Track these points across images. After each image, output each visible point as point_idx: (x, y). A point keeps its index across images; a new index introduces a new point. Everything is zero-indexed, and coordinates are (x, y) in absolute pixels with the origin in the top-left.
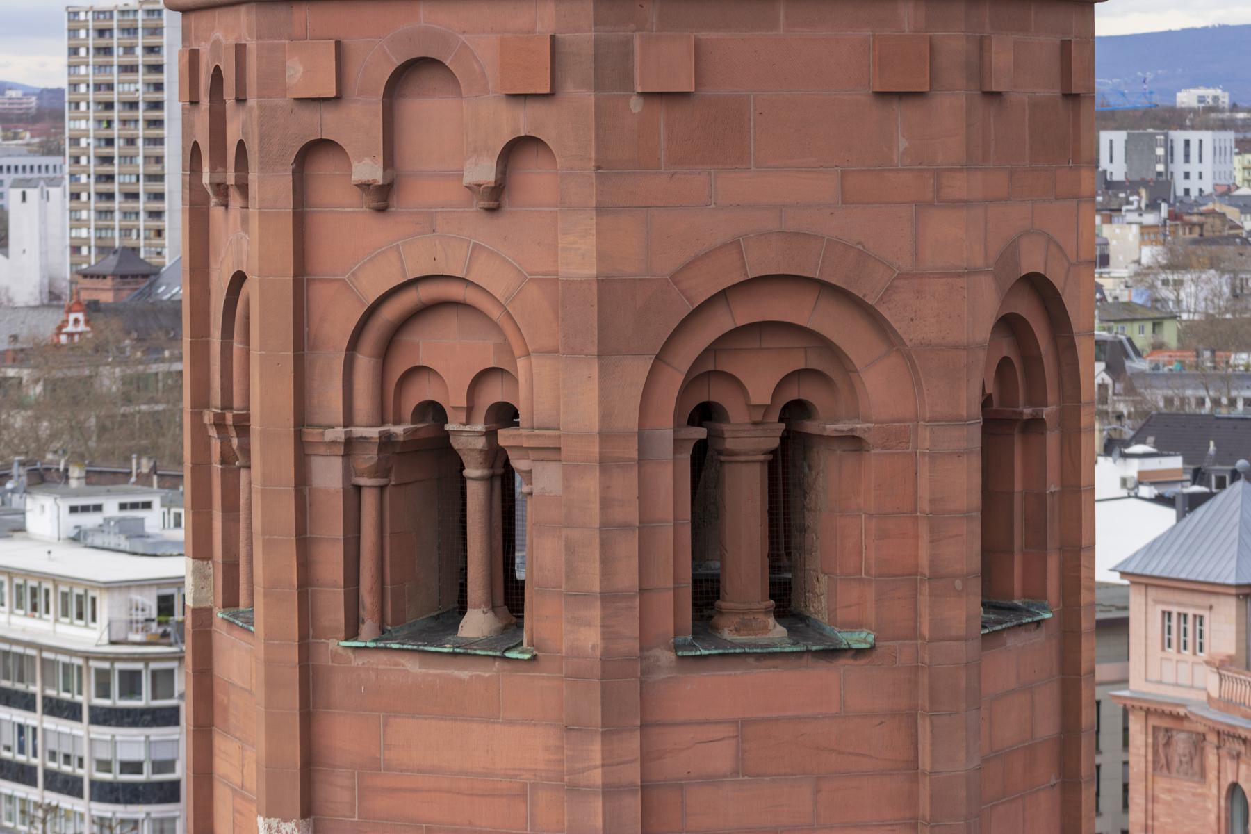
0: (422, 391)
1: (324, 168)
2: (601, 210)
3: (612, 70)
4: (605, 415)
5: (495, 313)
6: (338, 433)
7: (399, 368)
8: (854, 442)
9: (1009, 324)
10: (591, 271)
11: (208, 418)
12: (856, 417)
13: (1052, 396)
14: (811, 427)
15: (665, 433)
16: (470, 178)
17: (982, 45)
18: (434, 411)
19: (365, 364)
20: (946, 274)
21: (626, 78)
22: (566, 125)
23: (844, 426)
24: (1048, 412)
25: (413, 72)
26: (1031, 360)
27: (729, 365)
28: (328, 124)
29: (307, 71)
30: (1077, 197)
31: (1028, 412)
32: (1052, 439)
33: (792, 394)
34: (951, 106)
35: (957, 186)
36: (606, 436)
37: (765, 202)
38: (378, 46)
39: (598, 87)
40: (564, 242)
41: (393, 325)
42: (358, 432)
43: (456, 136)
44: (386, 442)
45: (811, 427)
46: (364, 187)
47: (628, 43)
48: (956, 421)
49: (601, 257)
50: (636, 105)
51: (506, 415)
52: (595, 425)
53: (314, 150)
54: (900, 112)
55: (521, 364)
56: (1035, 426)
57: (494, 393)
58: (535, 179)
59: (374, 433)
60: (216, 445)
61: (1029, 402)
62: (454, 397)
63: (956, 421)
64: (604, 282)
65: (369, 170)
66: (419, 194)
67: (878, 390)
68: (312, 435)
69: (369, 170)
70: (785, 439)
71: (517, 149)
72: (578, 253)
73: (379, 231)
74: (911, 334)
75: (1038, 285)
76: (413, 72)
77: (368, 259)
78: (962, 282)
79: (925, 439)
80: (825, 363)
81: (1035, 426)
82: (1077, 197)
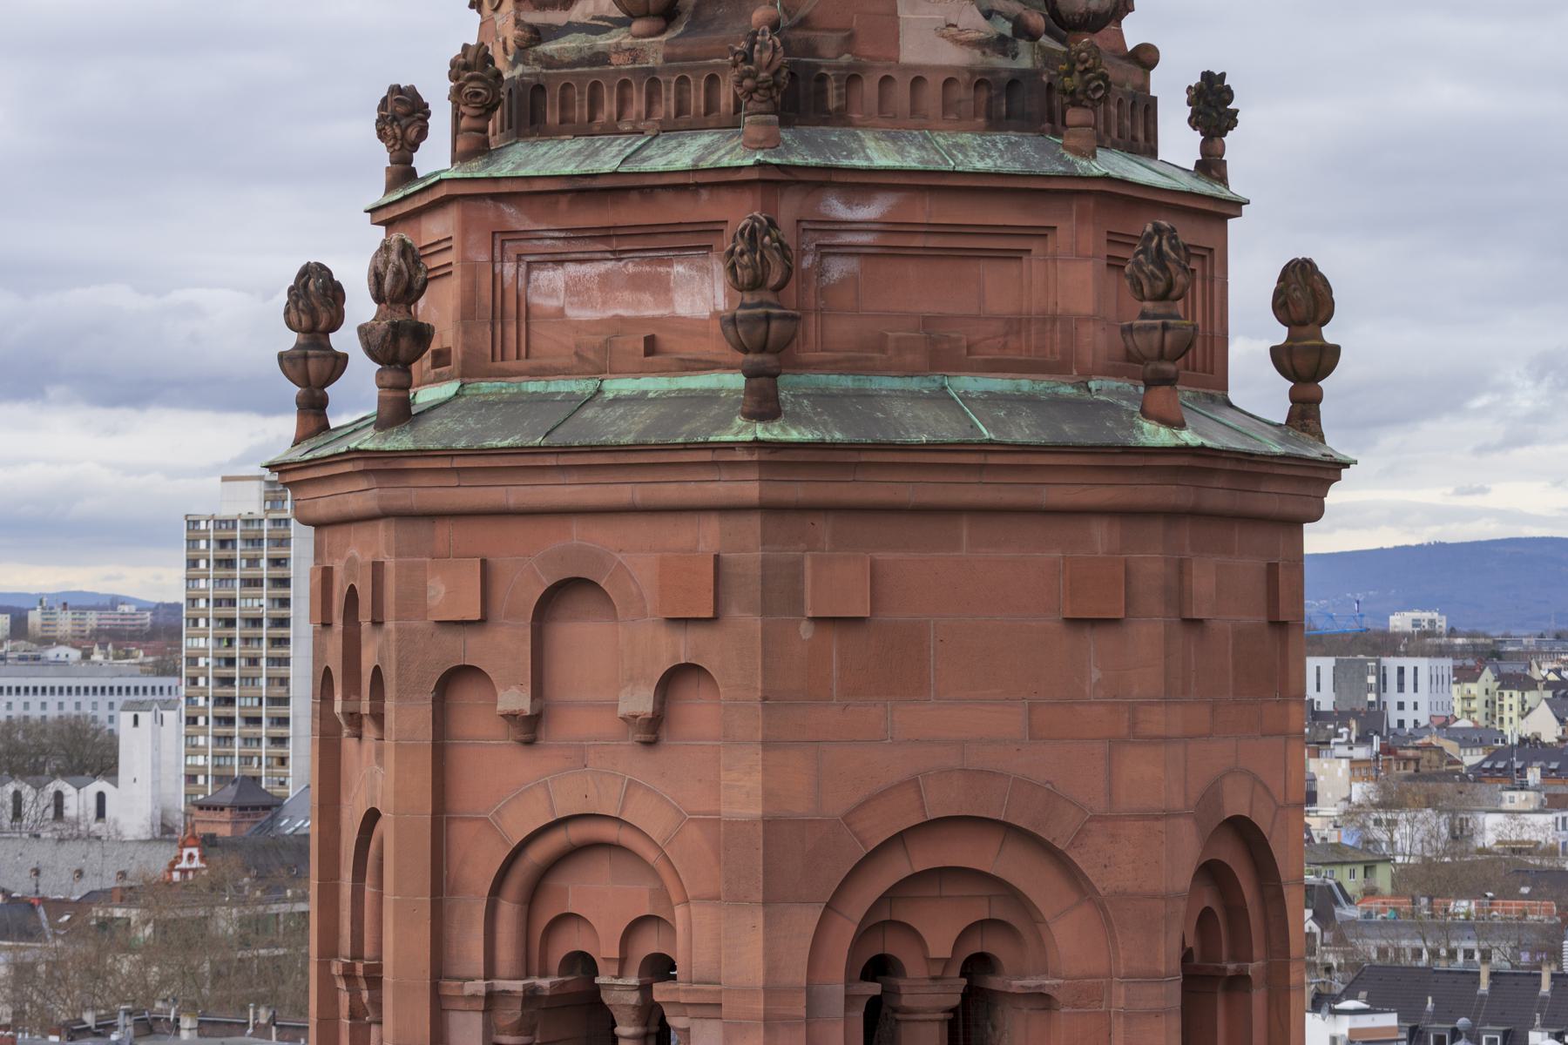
0: (570, 941)
1: (467, 697)
2: (767, 744)
3: (780, 593)
4: (771, 969)
5: (651, 856)
6: (479, 987)
7: (545, 916)
8: (1042, 1000)
9: (1211, 872)
10: (755, 811)
11: (336, 968)
12: (1045, 972)
13: (1257, 952)
14: (994, 983)
15: (835, 986)
16: (625, 709)
17: (1182, 568)
18: (583, 963)
19: (508, 910)
20: (1143, 817)
21: (796, 602)
22: (730, 652)
23: (1031, 982)
24: (1254, 968)
25: (566, 593)
26: (1236, 912)
27: (904, 914)
28: (471, 650)
29: (449, 591)
30: (1285, 734)
31: (1231, 967)
32: (1258, 997)
33: (975, 946)
34: (1148, 635)
35: (1156, 721)
36: (770, 991)
37: (948, 738)
38: (526, 569)
39: (766, 610)
40: (727, 780)
41: (542, 868)
42: (501, 985)
43: (610, 664)
44: (531, 995)
45: (994, 983)
46: (510, 717)
47: (798, 564)
48: (1153, 978)
49: (768, 795)
50: (806, 631)
51: (662, 967)
52: (758, 978)
53: (457, 677)
54: (1093, 641)
55: (679, 912)
56: (1239, 982)
57: (650, 944)
58: (697, 712)
59: (517, 986)
60: (344, 999)
61: (1234, 958)
62: (605, 948)
63: (1153, 978)
64: (770, 823)
65: (516, 699)
66: (570, 726)
67: (1069, 943)
68: (450, 988)
69: (516, 699)
70: (966, 996)
71: (677, 677)
72: (743, 792)
73: (522, 766)
74: (1104, 884)
75: (1243, 830)
76: (566, 593)
77: (515, 796)
78: (1160, 825)
79: (1120, 997)
80: (1011, 912)
81: (1239, 982)
82: (1285, 734)
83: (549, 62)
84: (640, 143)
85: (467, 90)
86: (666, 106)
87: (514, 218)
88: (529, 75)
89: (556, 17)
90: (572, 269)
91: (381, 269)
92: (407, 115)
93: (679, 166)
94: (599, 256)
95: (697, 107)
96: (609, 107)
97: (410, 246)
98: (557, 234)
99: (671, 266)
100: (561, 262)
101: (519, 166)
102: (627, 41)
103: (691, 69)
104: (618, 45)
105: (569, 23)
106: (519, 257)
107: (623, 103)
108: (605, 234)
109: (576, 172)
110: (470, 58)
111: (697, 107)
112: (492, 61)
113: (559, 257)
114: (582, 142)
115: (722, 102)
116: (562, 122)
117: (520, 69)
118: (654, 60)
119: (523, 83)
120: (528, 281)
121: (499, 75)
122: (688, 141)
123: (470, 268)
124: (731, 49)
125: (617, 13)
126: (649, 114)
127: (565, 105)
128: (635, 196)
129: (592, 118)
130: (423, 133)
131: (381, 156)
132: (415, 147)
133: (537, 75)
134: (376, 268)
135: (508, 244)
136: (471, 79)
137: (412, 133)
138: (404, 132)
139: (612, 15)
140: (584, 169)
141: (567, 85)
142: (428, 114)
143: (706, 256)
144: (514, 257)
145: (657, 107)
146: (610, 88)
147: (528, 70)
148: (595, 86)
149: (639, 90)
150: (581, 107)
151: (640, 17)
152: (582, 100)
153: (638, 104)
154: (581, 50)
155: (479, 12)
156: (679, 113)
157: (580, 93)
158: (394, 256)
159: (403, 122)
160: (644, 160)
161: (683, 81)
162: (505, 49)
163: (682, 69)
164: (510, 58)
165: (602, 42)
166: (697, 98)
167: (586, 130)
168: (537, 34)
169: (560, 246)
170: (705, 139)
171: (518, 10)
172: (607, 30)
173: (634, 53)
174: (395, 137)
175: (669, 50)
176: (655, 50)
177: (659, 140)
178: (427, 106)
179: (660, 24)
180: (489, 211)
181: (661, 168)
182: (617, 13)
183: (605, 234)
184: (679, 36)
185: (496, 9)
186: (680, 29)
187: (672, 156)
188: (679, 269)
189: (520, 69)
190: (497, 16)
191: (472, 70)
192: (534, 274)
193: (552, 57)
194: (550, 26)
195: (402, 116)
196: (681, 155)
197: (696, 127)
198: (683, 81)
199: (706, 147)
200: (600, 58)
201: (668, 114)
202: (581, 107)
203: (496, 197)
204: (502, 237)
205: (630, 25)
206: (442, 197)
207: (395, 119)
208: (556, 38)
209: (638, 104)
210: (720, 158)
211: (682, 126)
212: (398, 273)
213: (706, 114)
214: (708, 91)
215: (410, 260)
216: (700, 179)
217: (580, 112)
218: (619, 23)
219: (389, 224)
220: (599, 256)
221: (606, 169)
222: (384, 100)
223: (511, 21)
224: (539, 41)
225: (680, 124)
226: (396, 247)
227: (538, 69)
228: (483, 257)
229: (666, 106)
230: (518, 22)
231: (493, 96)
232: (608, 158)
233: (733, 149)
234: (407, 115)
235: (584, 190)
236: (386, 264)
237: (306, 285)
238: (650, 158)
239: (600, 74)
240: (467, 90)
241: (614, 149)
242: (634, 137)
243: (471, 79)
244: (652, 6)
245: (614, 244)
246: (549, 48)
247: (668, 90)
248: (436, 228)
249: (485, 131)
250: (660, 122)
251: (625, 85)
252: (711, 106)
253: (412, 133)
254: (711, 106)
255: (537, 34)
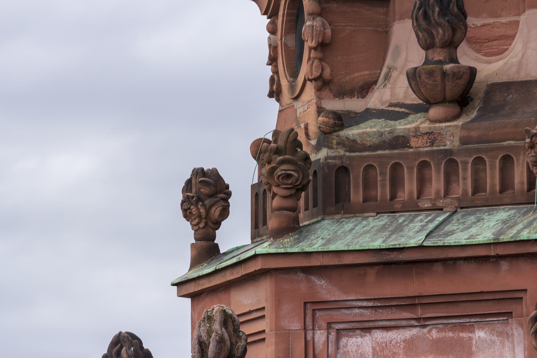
83: (352, 145)
84: (440, 219)
85: (279, 172)
86: (464, 184)
87: (325, 289)
88: (334, 158)
89: (354, 105)
90: (379, 335)
91: (204, 338)
92: (211, 196)
93: (480, 239)
94: (404, 323)
95: (493, 185)
96: (409, 186)
97: (231, 316)
98: (365, 304)
99: (473, 331)
100: (368, 330)
101: (329, 242)
102: (426, 126)
103: (487, 151)
104: (417, 129)
105: (368, 110)
106: (329, 325)
107: (422, 182)
108: (410, 303)
109: (384, 246)
110: (281, 143)
111: (493, 185)
112: (300, 145)
113: (367, 325)
114: (384, 219)
115: (517, 180)
116: (365, 201)
117: (324, 153)
118: (451, 143)
119: (328, 166)
120: (338, 348)
121: (307, 158)
122: (485, 216)
123: (283, 336)
124: (528, 132)
125: (413, 99)
126: (447, 193)
127: (368, 184)
128: (438, 268)
129: (393, 197)
130: (225, 213)
131: (186, 234)
132: (217, 224)
133: (341, 158)
134: (200, 337)
135: (318, 314)
136: (283, 162)
137: (216, 212)
138: (208, 211)
139: (408, 102)
140: (392, 243)
141: (370, 166)
142: (229, 194)
143: (506, 323)
144: (324, 325)
145: (454, 185)
146: (410, 169)
147: (332, 153)
148: (396, 168)
149: (438, 171)
150: (383, 186)
151: (437, 103)
152: (384, 180)
153: (436, 183)
154: (381, 134)
155: (278, 100)
156: (476, 191)
157: (383, 174)
158: (216, 326)
159: (207, 202)
160: (447, 234)
161: (479, 161)
162: (307, 134)
163: (478, 150)
164: (313, 142)
165: (402, 127)
166: (493, 177)
167: (388, 207)
168: (341, 120)
169: (368, 314)
170: (502, 214)
171: (319, 98)
172: (404, 116)
173: (432, 137)
174: (200, 216)
175: (465, 133)
176: (452, 132)
177: (455, 217)
178: (227, 187)
179: (455, 109)
180: (301, 285)
181: (464, 242)
182: (413, 99)
183: (410, 303)
184: (473, 121)
185: (297, 98)
186: (474, 114)
187: (473, 230)
188: (480, 334)
189: (324, 153)
190: (297, 104)
191: (277, 154)
192: (344, 341)
193: (354, 141)
194: (349, 112)
195: (205, 197)
196: (483, 228)
197: (493, 204)
198: (479, 161)
199: (504, 222)
200: (400, 142)
201: (465, 192)
202: (383, 186)
203: (308, 270)
204: (314, 306)
205: (426, 110)
206: (250, 273)
207: (199, 199)
208: (357, 123)
209: (436, 183)
210: (519, 232)
211: (478, 203)
212: (221, 341)
213: (501, 192)
214: (503, 170)
215: (231, 329)
216: (501, 251)
217: (382, 190)
218: (415, 109)
219: (194, 296)
220: (404, 323)
221: (413, 243)
222: (189, 183)
223: (313, 109)
224: (342, 127)
225: (478, 200)
226: (218, 318)
227: (341, 152)
228: (296, 326)
229: (464, 184)
230: (320, 110)
231: (300, 179)
232: (413, 233)
233: (530, 224)
234: (211, 196)
235: (391, 263)
236: (209, 333)
237: (119, 353)
238: (452, 233)
239: (400, 156)
240: (279, 172)
241: (417, 225)
242: (434, 214)
243: (283, 162)
244: (448, 94)
245: (420, 312)
246: (352, 132)
247: (465, 170)
248: (243, 301)
249: (294, 209)
250: (458, 199)
251: (424, 166)
252: (506, 184)
253: (216, 212)
254: (506, 184)
255: (341, 120)
